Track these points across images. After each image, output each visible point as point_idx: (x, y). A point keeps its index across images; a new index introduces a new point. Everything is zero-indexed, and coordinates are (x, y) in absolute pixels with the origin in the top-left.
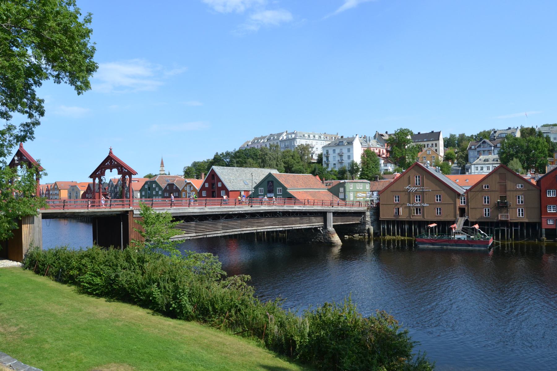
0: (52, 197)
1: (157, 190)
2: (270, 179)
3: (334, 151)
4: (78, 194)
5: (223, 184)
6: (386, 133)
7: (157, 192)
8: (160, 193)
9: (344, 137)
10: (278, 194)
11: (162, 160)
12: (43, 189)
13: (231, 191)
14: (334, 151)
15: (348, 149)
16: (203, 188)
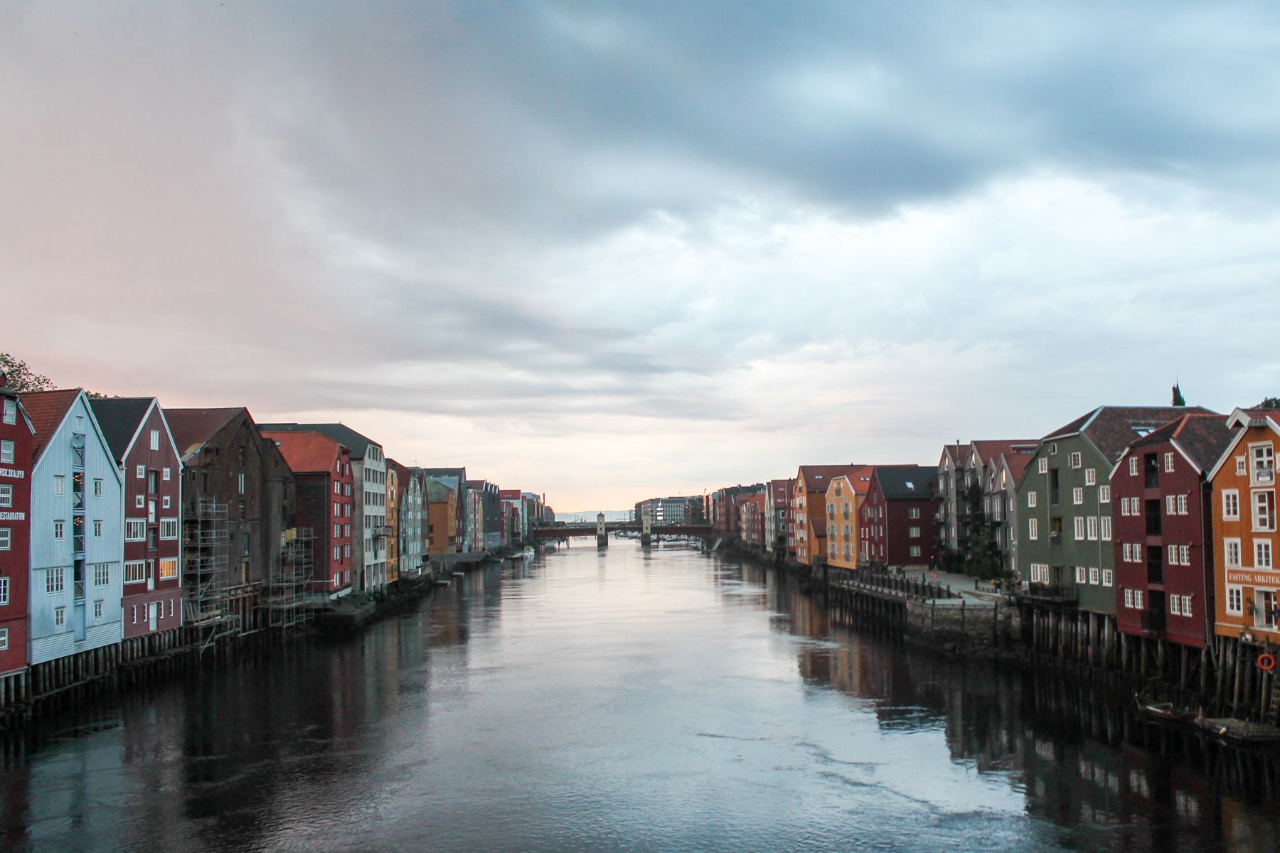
1: (1090, 479)
7: (1090, 493)
8: (1104, 497)
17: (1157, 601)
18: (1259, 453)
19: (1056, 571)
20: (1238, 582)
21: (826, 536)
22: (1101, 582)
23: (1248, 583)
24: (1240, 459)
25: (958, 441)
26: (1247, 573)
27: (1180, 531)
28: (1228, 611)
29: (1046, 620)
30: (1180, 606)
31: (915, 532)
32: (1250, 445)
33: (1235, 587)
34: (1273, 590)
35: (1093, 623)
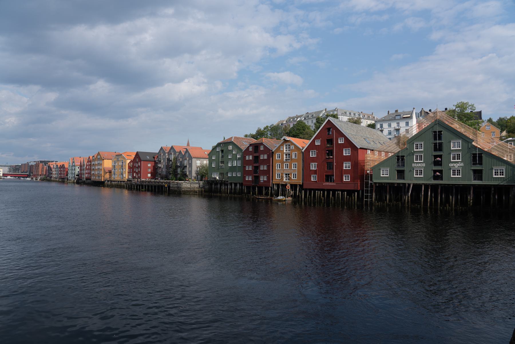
0: (93, 168)
2: (438, 129)
3: (390, 125)
4: (124, 164)
5: (346, 139)
6: (430, 111)
9: (399, 111)
10: (452, 149)
11: (188, 141)
12: (83, 160)
13: (360, 148)
14: (390, 125)
16: (312, 146)
17: (257, 178)
18: (286, 146)
19: (221, 174)
20: (280, 172)
21: (111, 172)
22: (237, 175)
23: (282, 172)
24: (281, 147)
25: (167, 145)
26: (282, 170)
27: (265, 162)
28: (277, 178)
29: (217, 186)
31: (150, 170)
32: (284, 144)
33: (278, 173)
34: (289, 173)
35: (233, 185)
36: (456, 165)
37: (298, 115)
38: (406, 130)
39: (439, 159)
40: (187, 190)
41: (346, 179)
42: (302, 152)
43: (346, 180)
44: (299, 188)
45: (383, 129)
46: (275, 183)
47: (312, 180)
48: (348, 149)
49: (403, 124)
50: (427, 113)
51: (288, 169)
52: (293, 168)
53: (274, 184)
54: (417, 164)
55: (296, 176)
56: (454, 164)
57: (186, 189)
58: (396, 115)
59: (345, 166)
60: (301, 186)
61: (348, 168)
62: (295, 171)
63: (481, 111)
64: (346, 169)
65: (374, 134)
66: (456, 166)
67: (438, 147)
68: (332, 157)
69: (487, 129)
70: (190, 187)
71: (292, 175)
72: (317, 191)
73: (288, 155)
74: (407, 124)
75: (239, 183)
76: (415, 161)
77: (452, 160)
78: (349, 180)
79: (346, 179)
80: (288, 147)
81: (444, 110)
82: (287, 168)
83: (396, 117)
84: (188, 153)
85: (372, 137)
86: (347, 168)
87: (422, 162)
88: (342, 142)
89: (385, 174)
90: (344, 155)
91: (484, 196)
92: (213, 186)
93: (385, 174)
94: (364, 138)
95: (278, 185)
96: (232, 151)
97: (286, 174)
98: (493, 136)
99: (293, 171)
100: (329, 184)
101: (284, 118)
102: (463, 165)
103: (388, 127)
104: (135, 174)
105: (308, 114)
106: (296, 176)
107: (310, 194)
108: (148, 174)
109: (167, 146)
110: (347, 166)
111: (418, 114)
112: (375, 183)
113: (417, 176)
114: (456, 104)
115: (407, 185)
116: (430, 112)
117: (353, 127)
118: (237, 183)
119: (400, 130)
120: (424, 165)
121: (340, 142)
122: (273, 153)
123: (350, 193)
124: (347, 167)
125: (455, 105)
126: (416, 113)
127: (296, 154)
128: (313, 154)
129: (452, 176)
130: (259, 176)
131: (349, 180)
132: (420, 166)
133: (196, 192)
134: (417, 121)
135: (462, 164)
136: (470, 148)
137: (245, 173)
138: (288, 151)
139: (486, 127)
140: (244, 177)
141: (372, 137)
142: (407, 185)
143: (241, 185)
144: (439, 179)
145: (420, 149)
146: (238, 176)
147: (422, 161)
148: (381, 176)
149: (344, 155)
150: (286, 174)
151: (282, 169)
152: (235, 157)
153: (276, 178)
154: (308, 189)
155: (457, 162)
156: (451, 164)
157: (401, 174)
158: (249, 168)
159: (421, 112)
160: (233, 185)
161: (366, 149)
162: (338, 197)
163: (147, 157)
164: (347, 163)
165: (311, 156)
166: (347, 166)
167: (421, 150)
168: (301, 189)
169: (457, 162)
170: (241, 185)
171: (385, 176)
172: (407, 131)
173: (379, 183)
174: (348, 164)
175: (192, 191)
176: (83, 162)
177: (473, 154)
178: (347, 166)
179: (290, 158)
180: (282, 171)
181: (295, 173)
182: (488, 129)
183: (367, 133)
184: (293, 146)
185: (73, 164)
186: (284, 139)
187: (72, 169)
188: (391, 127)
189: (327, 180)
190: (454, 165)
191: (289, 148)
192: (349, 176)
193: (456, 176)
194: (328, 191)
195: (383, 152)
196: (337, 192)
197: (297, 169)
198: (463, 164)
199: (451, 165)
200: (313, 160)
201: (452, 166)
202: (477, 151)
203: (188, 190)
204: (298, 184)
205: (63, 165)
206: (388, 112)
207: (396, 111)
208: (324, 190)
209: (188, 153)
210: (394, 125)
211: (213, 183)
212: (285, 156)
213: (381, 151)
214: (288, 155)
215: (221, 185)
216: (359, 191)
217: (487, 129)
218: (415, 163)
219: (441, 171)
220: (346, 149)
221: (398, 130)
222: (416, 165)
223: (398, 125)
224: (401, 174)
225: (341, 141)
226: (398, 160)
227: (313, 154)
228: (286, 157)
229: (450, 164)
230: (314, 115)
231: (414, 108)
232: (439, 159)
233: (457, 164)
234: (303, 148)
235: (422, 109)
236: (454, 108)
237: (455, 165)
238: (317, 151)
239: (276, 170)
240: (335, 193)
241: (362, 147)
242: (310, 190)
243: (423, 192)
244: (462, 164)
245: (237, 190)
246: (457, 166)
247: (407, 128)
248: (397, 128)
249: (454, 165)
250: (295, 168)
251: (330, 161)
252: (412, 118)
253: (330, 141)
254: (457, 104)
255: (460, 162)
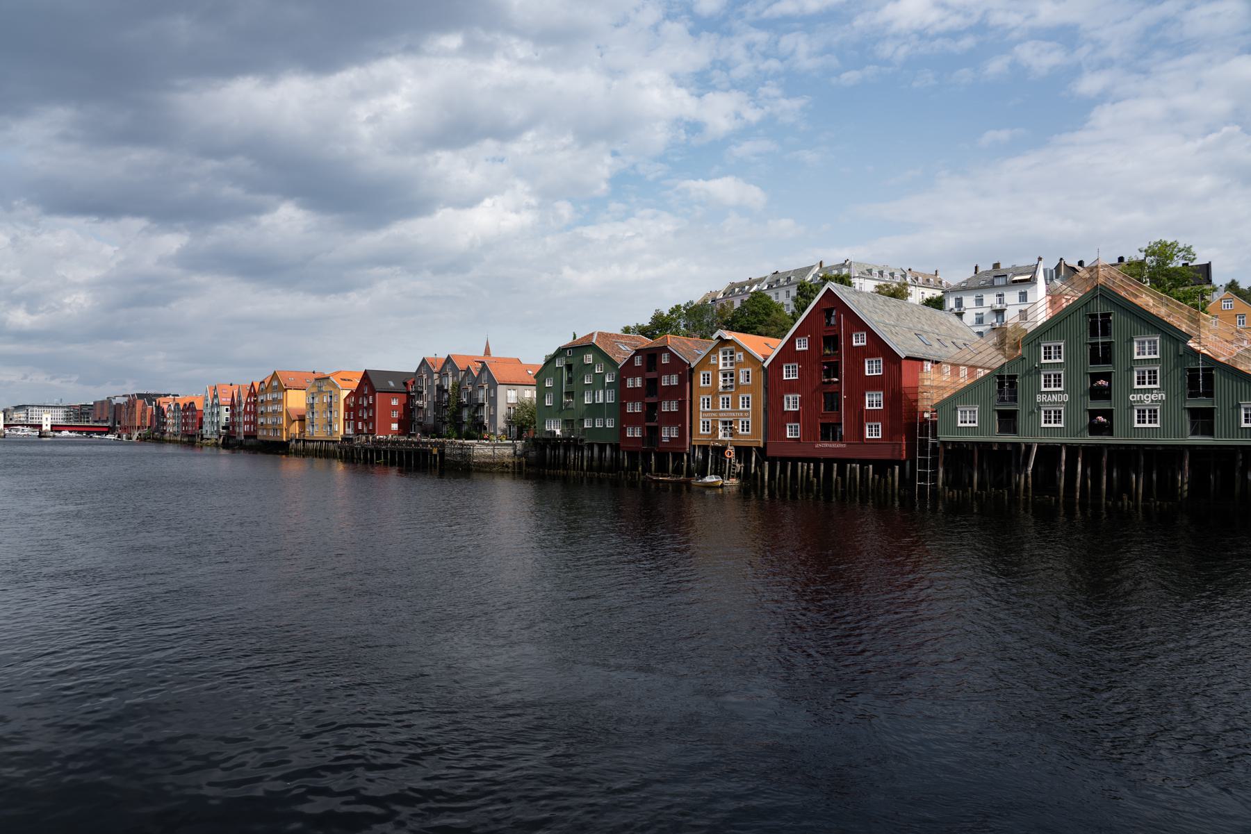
0: (263, 409)
2: (1100, 308)
3: (980, 301)
4: (334, 399)
5: (872, 335)
6: (1081, 263)
9: (1002, 267)
10: (1136, 357)
11: (487, 342)
12: (239, 391)
13: (907, 358)
14: (980, 301)
15: (1020, 293)
16: (787, 354)
17: (653, 433)
18: (725, 353)
19: (567, 423)
21: (304, 420)
22: (605, 425)
24: (712, 356)
26: (713, 412)
27: (671, 393)
28: (701, 432)
30: (668, 433)
31: (395, 415)
33: (706, 420)
34: (731, 419)
35: (596, 450)
36: (1148, 397)
37: (754, 277)
38: (1020, 311)
39: (1102, 382)
40: (484, 463)
41: (872, 432)
42: (763, 367)
43: (872, 435)
44: (756, 456)
45: (962, 309)
46: (697, 444)
47: (788, 436)
48: (876, 361)
49: (1011, 297)
50: (1074, 269)
51: (730, 409)
52: (741, 408)
53: (695, 446)
54: (1049, 396)
55: (748, 426)
56: (1142, 395)
57: (483, 460)
58: (996, 277)
59: (869, 401)
60: (762, 451)
61: (876, 406)
62: (746, 414)
63: (1210, 263)
64: (871, 408)
65: (941, 324)
66: (1148, 399)
67: (1102, 355)
68: (836, 380)
69: (1224, 307)
70: (491, 453)
71: (738, 425)
72: (800, 464)
73: (728, 375)
74: (1023, 297)
75: (611, 445)
76: (1043, 389)
77: (1136, 386)
78: (880, 437)
79: (872, 432)
80: (728, 356)
81: (1116, 261)
82: (728, 407)
83: (996, 280)
84: (486, 373)
85: (937, 331)
86: (875, 408)
87: (1060, 392)
88: (863, 344)
89: (968, 422)
90: (867, 374)
91: (1218, 473)
92: (548, 450)
93: (968, 422)
94: (917, 332)
95: (705, 449)
96: (591, 367)
97: (725, 423)
98: (1240, 324)
99: (742, 414)
100: (830, 446)
101: (720, 287)
102: (1164, 398)
103: (976, 305)
104: (360, 424)
105: (777, 274)
106: (748, 426)
107: (783, 470)
108: (392, 424)
109: (437, 356)
110: (873, 400)
111: (1051, 271)
112: (944, 443)
113: (1048, 425)
114: (1146, 248)
115: (1023, 448)
116: (1080, 267)
117: (888, 306)
118: (606, 445)
119: (1006, 313)
120: (1066, 398)
121: (857, 344)
122: (692, 370)
123: (882, 466)
124: (875, 405)
125: (1144, 249)
126: (1045, 271)
127: (748, 372)
128: (789, 373)
129: (1136, 425)
130: (657, 427)
131: (880, 437)
132: (1056, 400)
133: (507, 466)
134: (1047, 291)
135: (1162, 396)
136: (1181, 356)
137: (625, 420)
138: (728, 367)
139: (1223, 303)
140: (623, 431)
141: (937, 331)
142: (1023, 448)
143: (616, 448)
144: (1104, 433)
145: (1055, 358)
146: (607, 426)
147: (1061, 389)
148: (960, 425)
149: (867, 374)
150: (725, 423)
151: (715, 410)
152: (599, 382)
153: (699, 431)
154: (779, 457)
155: (1150, 391)
156: (1135, 396)
157: (1008, 420)
158: (635, 408)
159: (1058, 268)
160: (596, 450)
161: (922, 360)
162: (853, 478)
163: (390, 382)
164: (874, 393)
165: (785, 378)
166: (875, 403)
167: (1058, 361)
168: (760, 458)
169: (1150, 391)
170: (616, 448)
171: (968, 425)
172: (1023, 314)
173: (953, 443)
174: (876, 397)
175: (497, 463)
176: (239, 396)
177: (1190, 370)
178: (875, 403)
179: (734, 384)
180: (714, 415)
181: (745, 420)
182: (1228, 307)
183: (923, 320)
184: (741, 354)
185: (216, 401)
186: (719, 337)
187: (213, 413)
188: (982, 305)
189: (825, 437)
190: (1141, 397)
191: (731, 358)
192: (878, 427)
193: (1147, 425)
194: (829, 462)
195: (964, 365)
196: (851, 466)
197: (750, 408)
198: (1164, 395)
199: (1133, 397)
200: (791, 387)
201: (1135, 399)
202: (1201, 362)
203: (487, 460)
204: (755, 447)
205: (190, 403)
206: (976, 267)
207: (996, 266)
208: (817, 461)
209: (486, 373)
210: (990, 299)
211: (548, 446)
212: (721, 378)
213: (958, 365)
214: (728, 375)
215: (567, 448)
216: (904, 462)
217: (1224, 307)
218: (1044, 392)
219: (1108, 414)
220: (870, 360)
221: (999, 313)
222: (1047, 399)
223: (1000, 299)
224: (1008, 420)
225: (859, 341)
226: (1001, 385)
227: (789, 373)
228: (725, 381)
229: (1132, 395)
230: (792, 278)
231: (1040, 259)
232: (1102, 382)
233: (1150, 395)
234: (766, 359)
235: (1061, 259)
236: (1141, 256)
237: (1144, 397)
238: (800, 366)
239: (699, 411)
240: (846, 467)
241: (910, 354)
242: (784, 460)
243: (1063, 463)
244: (1162, 396)
245: (605, 460)
246: (1150, 401)
247: (1023, 307)
248: (998, 306)
249: (1141, 397)
250: (746, 408)
251: (830, 389)
252: (1036, 283)
253: (832, 341)
254: (1149, 247)
255: (1156, 389)
